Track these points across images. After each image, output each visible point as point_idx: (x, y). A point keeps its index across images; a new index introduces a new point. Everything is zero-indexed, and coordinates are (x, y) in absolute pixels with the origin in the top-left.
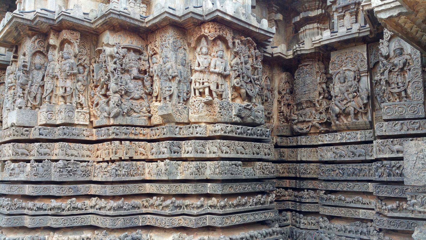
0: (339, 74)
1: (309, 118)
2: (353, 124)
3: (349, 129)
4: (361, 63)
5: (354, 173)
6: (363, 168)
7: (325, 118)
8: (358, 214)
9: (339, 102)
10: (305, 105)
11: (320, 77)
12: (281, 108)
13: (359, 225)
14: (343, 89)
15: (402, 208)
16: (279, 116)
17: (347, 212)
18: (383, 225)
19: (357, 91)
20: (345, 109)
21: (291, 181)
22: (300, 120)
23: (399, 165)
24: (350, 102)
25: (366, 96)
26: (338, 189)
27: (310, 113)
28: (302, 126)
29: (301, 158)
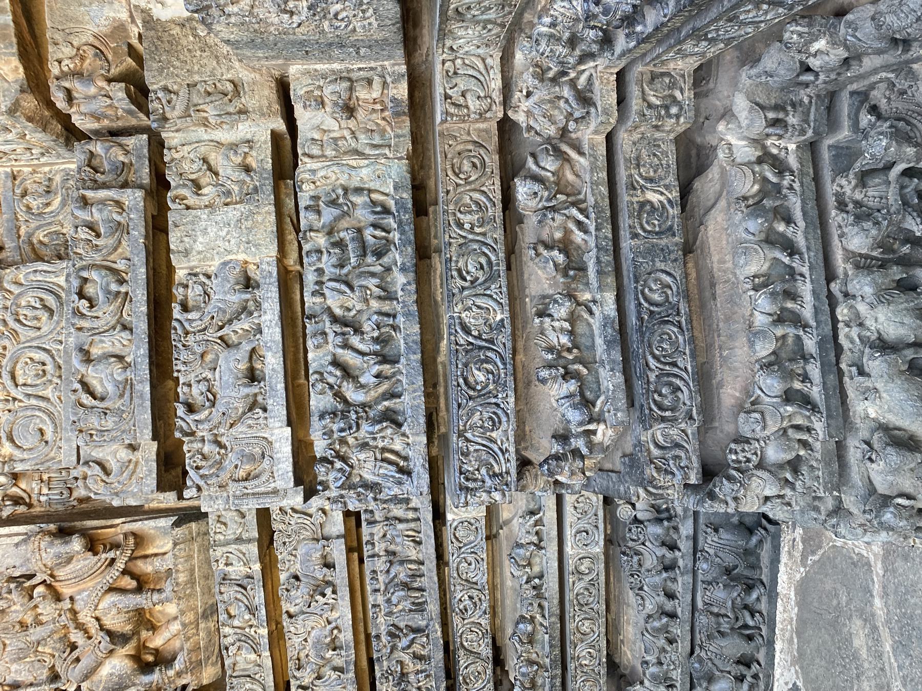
2: (190, 595)
5: (406, 586)
6: (383, 546)
9: (78, 660)
15: (569, 350)
17: (585, 608)
18: (678, 446)
19: (27, 584)
20: (109, 633)
23: (331, 368)
24: (74, 612)
25: (51, 543)
26: (486, 651)
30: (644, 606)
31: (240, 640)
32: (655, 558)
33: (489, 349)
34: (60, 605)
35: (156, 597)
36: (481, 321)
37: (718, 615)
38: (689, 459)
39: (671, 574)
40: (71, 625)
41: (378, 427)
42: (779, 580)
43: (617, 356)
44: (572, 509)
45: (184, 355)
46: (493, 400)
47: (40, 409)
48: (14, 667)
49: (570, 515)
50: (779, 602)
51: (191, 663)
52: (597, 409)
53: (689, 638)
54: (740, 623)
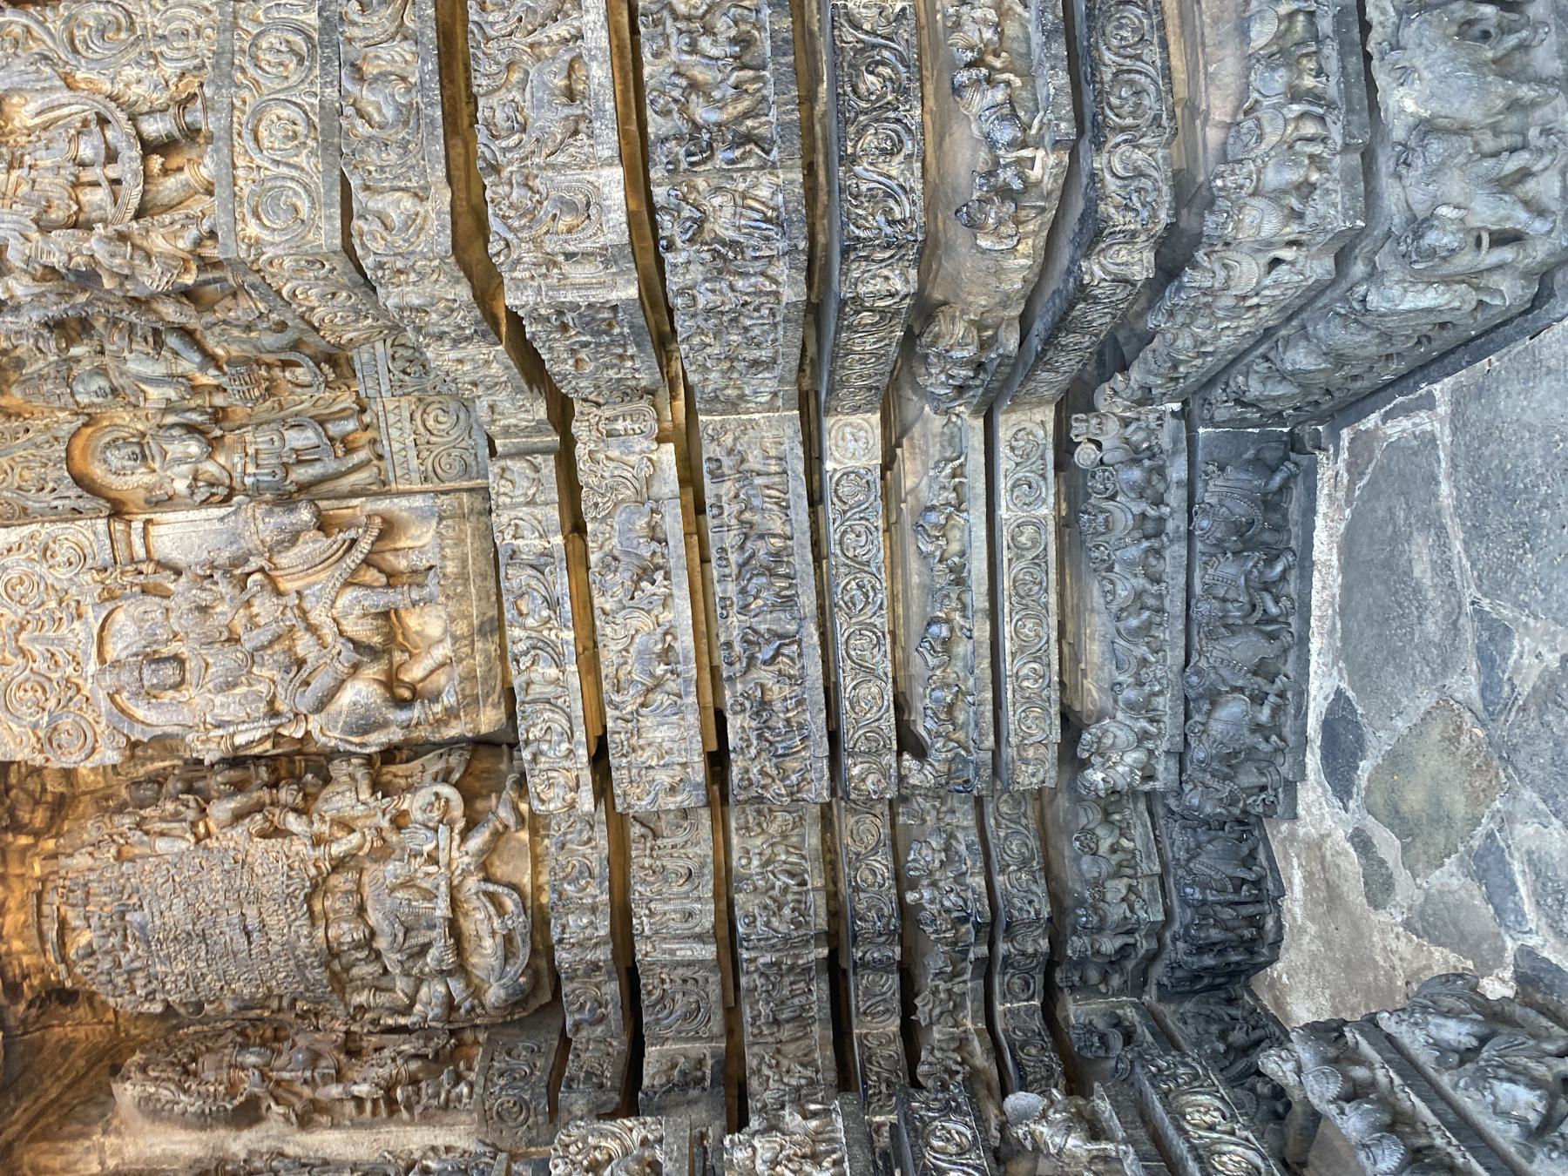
0: (122, 698)
1: (430, 896)
2: (462, 596)
3: (495, 626)
4: (59, 559)
7: (437, 795)
8: (1030, 530)
10: (346, 932)
11: (162, 834)
12: (359, 1101)
13: (1101, 518)
14: (222, 661)
16: (418, 1110)
21: (857, 1002)
22: (450, 958)
24: (304, 614)
25: (270, 513)
27: (400, 894)
28: (488, 943)
29: (699, 938)
30: (1114, 593)
31: (534, 648)
32: (1130, 517)
33: (886, 47)
34: (284, 600)
35: (415, 595)
36: (875, 11)
37: (1224, 600)
38: (1158, 190)
39: (1155, 543)
40: (302, 625)
41: (738, 153)
42: (1316, 541)
43: (1059, 48)
44: (1007, 451)
45: (487, 67)
46: (892, 115)
47: (292, 179)
48: (219, 699)
49: (1005, 460)
50: (1316, 573)
51: (464, 697)
52: (1033, 131)
53: (1182, 643)
54: (1258, 615)
